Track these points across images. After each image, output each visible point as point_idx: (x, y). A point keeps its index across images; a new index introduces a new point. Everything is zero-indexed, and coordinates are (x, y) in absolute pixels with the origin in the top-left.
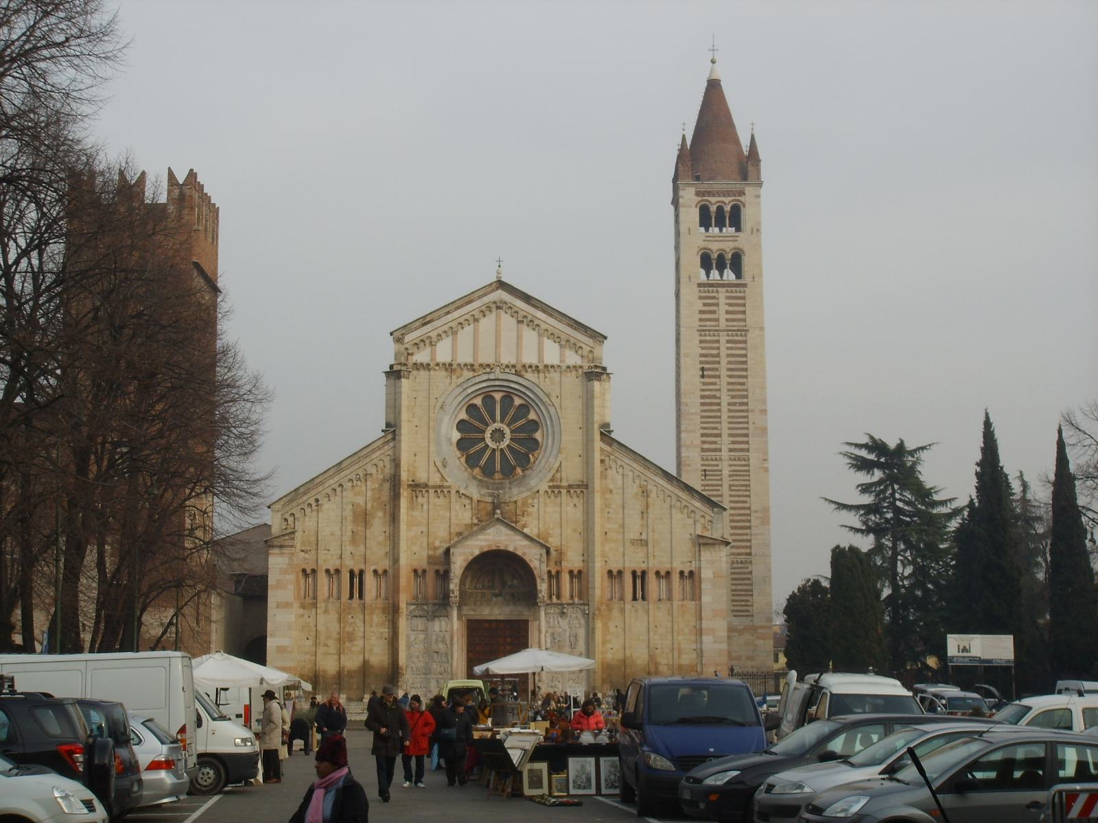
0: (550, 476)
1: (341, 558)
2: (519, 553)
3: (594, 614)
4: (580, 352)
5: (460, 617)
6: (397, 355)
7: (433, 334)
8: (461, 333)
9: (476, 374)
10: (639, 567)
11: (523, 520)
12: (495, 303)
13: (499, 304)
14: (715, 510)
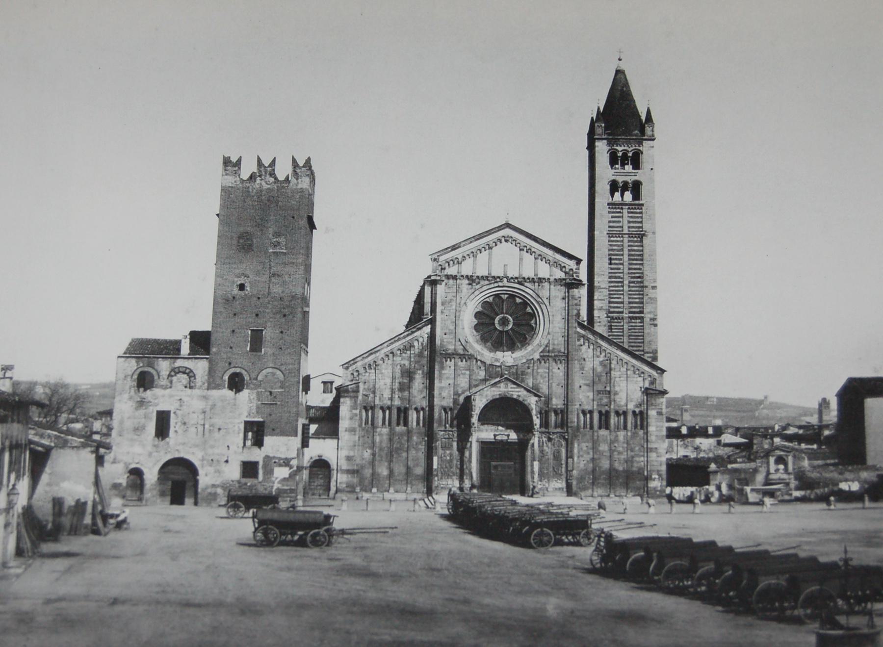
0: (541, 350)
7: (460, 257)
8: (479, 255)
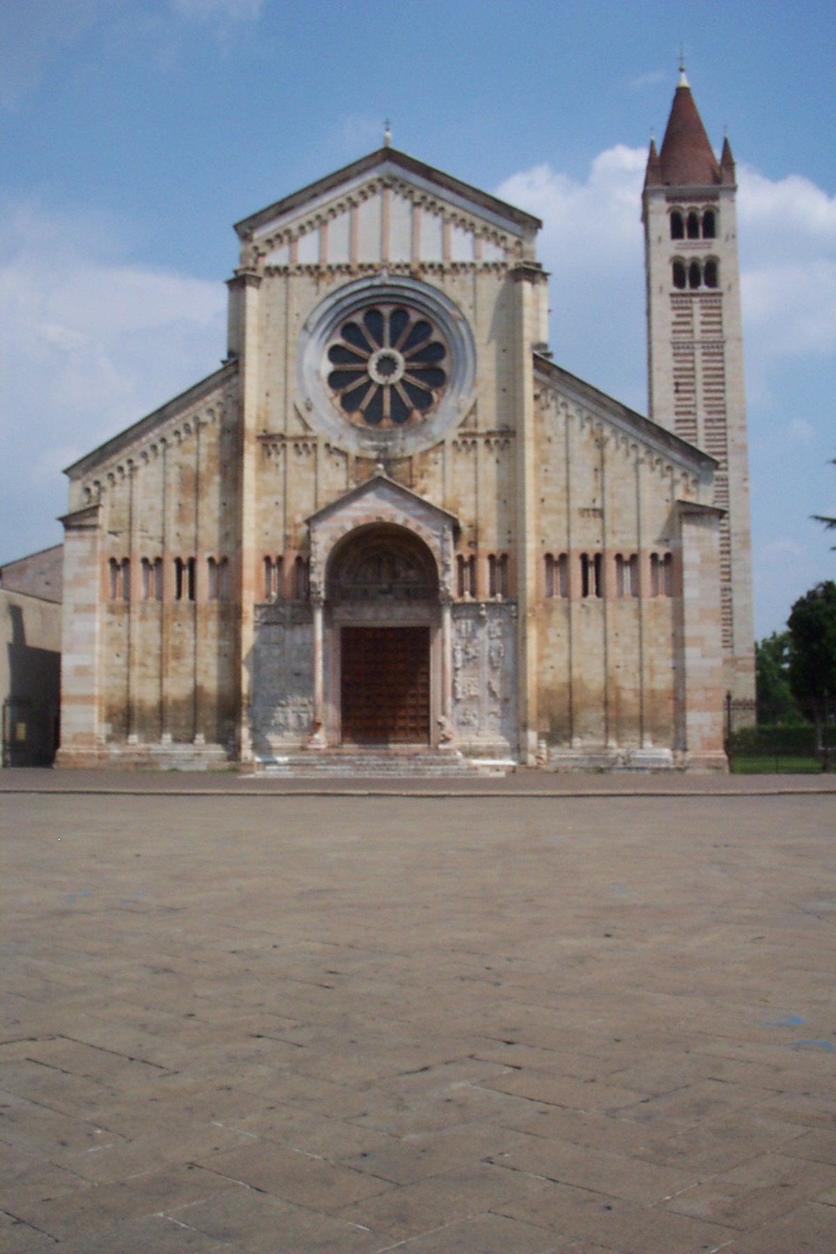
0: (460, 418)
3: (525, 616)
4: (502, 244)
5: (328, 622)
6: (243, 257)
7: (294, 227)
9: (353, 279)
10: (593, 549)
11: (421, 483)
14: (703, 464)
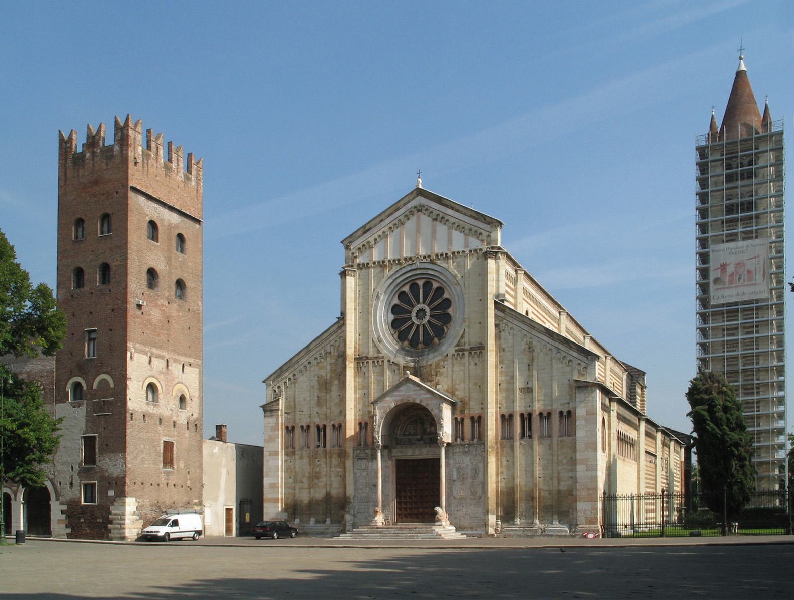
0: (456, 341)
1: (310, 417)
2: (424, 404)
7: (371, 240)
9: (402, 267)
12: (415, 207)
13: (418, 208)
14: (589, 357)
